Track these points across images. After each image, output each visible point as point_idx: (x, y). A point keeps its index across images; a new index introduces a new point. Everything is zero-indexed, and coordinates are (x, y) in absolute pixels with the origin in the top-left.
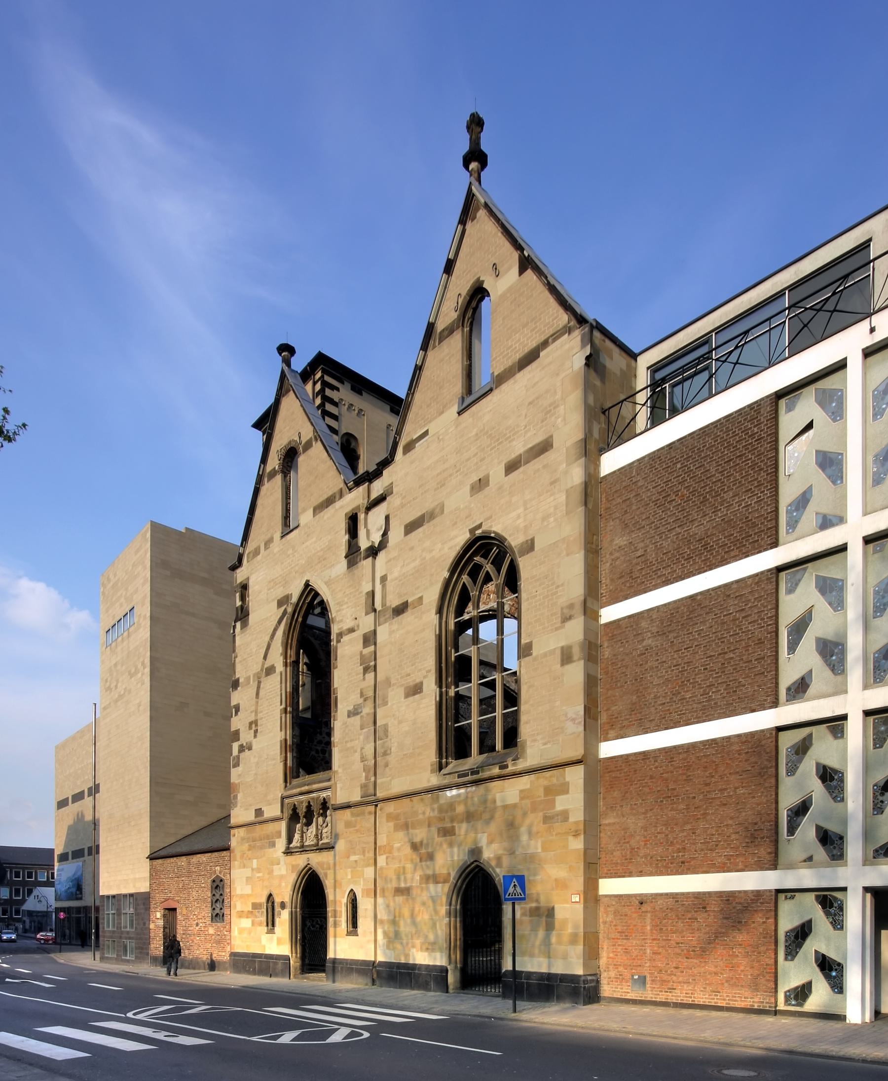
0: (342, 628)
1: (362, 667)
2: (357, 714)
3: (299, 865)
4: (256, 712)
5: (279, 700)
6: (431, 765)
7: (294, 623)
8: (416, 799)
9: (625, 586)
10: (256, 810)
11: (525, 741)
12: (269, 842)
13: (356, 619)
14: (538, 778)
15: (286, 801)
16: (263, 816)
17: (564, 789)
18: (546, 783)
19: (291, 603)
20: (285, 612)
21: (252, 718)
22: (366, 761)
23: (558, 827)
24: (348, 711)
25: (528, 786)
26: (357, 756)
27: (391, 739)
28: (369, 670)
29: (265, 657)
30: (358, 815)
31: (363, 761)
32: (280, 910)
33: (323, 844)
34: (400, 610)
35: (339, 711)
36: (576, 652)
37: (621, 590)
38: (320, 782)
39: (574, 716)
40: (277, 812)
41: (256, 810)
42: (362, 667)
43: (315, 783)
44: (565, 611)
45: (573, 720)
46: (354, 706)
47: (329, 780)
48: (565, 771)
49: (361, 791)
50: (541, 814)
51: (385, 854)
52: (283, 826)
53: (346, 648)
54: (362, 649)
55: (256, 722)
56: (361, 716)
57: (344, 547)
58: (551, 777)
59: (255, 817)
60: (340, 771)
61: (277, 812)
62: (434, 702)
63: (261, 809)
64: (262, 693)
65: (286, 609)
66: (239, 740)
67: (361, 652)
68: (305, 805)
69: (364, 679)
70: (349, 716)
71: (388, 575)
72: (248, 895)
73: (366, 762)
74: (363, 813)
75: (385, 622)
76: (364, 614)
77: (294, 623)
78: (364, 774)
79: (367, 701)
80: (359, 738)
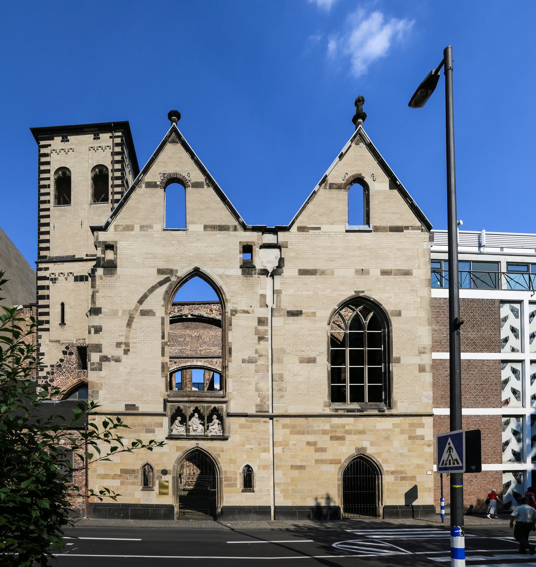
0: (237, 308)
1: (257, 336)
2: (253, 362)
3: (186, 447)
4: (127, 337)
5: (160, 335)
6: (324, 403)
7: (176, 289)
8: (310, 419)
9: (438, 346)
10: (126, 405)
11: (396, 401)
12: (146, 429)
13: (251, 307)
14: (405, 419)
15: (169, 404)
16: (138, 410)
17: (422, 426)
18: (410, 422)
19: (176, 276)
20: (167, 280)
21: (122, 339)
22: (261, 391)
23: (418, 442)
24: (242, 359)
25: (399, 422)
26: (252, 387)
27: (286, 383)
28: (264, 340)
29: (141, 302)
30: (254, 422)
31: (257, 391)
32: (161, 475)
33: (212, 436)
34: (293, 314)
35: (233, 357)
36: (428, 368)
37: (436, 348)
38: (212, 397)
39: (427, 395)
40: (160, 409)
41: (126, 405)
42: (257, 336)
43: (206, 397)
44: (421, 349)
45: (427, 397)
46: (249, 357)
47: (223, 397)
48: (422, 418)
49: (256, 408)
50: (407, 435)
51: (282, 446)
52: (166, 420)
53: (241, 321)
54: (257, 326)
55: (127, 344)
56: (256, 365)
57: (239, 261)
58: (414, 419)
59: (126, 410)
60: (234, 393)
61: (160, 409)
62: (326, 370)
63: (135, 405)
64: (134, 325)
65: (169, 277)
66: (100, 351)
67: (256, 328)
68: (192, 409)
69: (259, 344)
70: (243, 362)
71: (283, 291)
72: (119, 464)
73: (261, 392)
74: (259, 421)
75: (280, 316)
76: (259, 306)
77: (176, 289)
78: (259, 399)
79: (262, 357)
80: (254, 377)
